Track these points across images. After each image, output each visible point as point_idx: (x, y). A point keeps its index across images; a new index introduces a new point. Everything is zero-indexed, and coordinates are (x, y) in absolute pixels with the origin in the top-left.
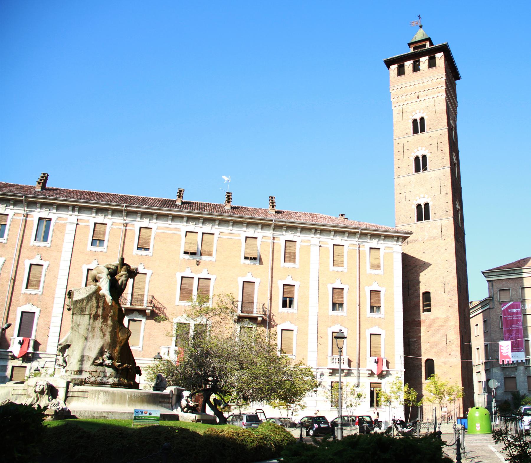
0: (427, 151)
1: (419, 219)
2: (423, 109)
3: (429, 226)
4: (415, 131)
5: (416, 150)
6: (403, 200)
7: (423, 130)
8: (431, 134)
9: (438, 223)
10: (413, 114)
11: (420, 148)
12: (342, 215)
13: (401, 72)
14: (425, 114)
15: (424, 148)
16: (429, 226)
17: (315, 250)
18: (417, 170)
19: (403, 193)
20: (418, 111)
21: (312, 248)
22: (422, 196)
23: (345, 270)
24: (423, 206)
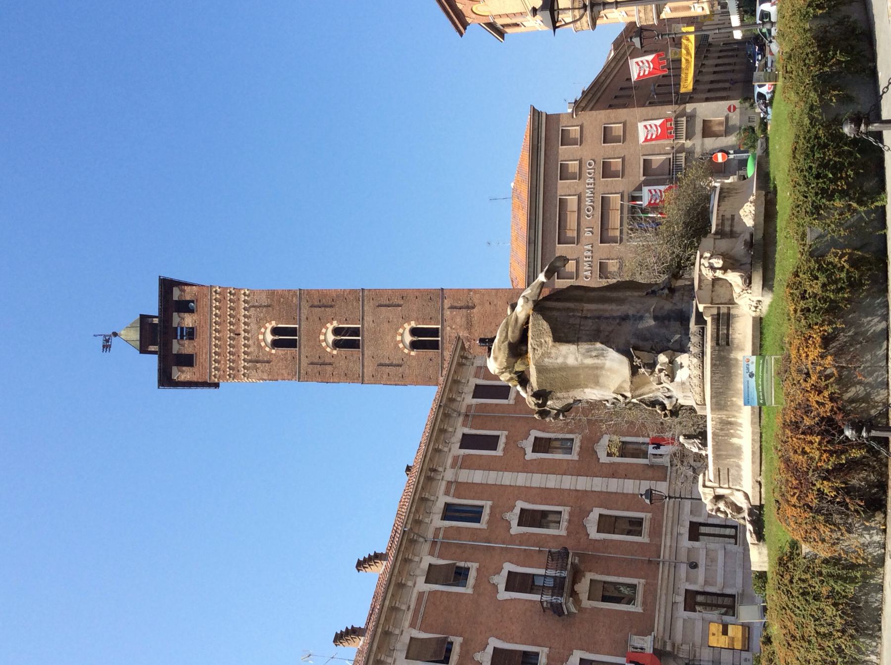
0: (328, 325)
1: (434, 346)
2: (260, 328)
3: (448, 328)
4: (292, 344)
5: (324, 344)
6: (401, 369)
7: (293, 332)
8: (303, 317)
9: (447, 313)
10: (263, 344)
11: (322, 337)
12: (408, 469)
13: (188, 360)
14: (267, 325)
15: (324, 330)
16: (448, 328)
17: (465, 476)
18: (354, 345)
19: (387, 370)
20: (261, 337)
21: (461, 479)
22: (399, 338)
23: (506, 433)
24: (415, 339)
